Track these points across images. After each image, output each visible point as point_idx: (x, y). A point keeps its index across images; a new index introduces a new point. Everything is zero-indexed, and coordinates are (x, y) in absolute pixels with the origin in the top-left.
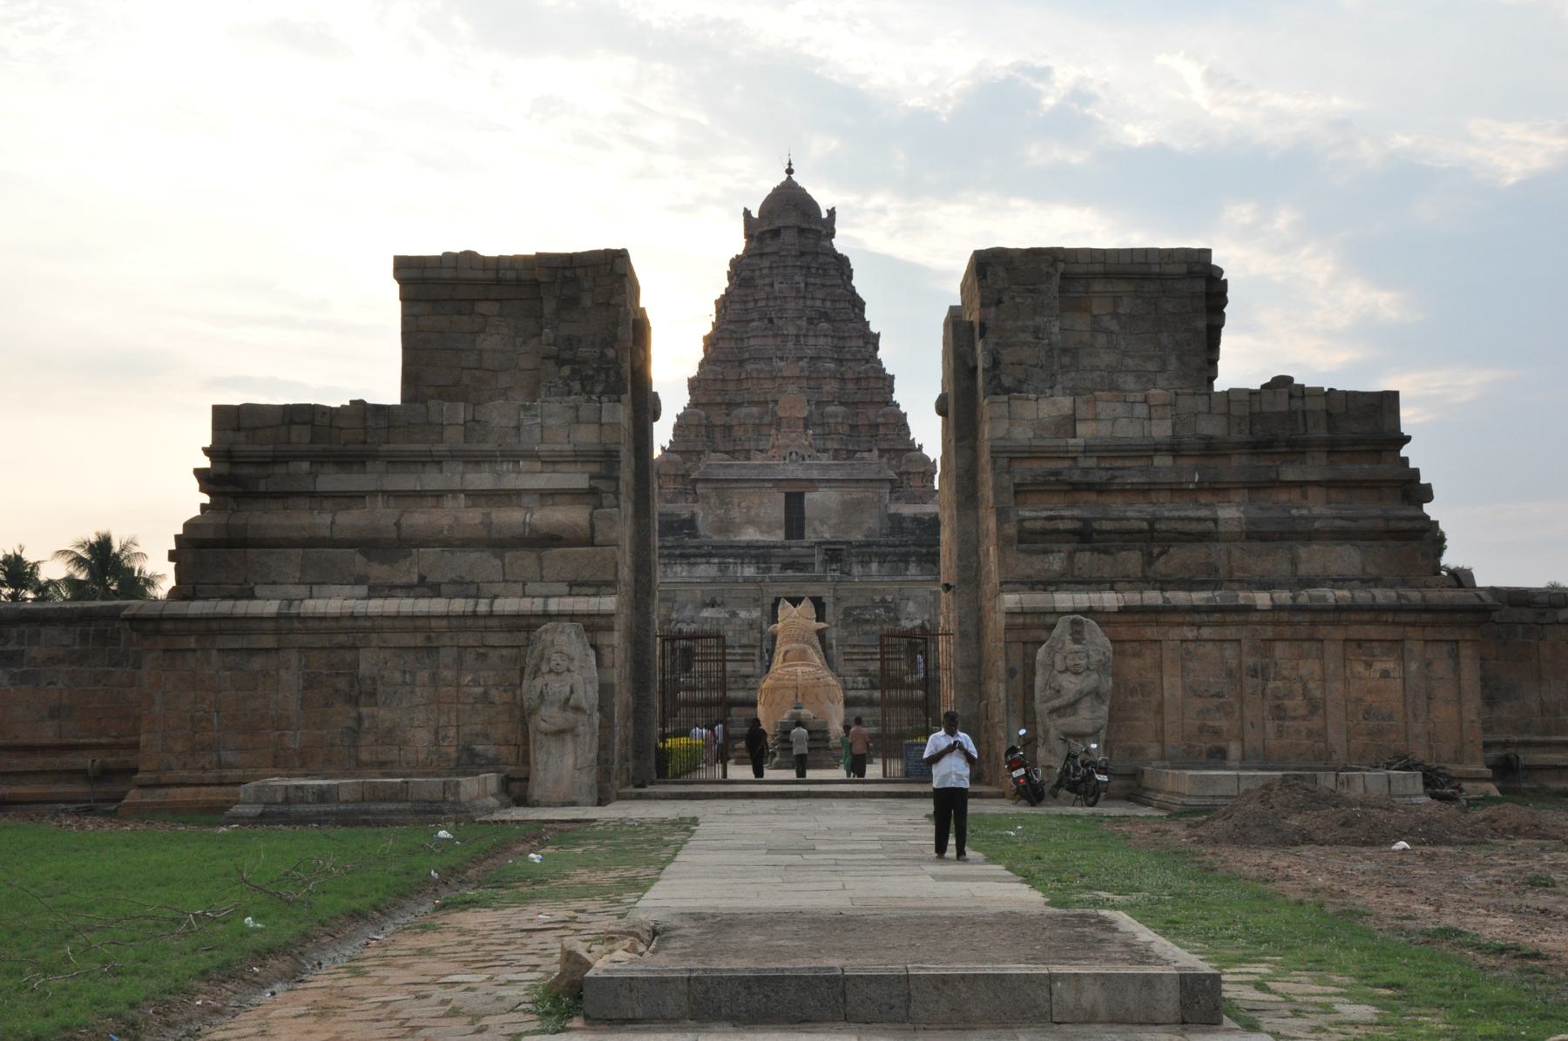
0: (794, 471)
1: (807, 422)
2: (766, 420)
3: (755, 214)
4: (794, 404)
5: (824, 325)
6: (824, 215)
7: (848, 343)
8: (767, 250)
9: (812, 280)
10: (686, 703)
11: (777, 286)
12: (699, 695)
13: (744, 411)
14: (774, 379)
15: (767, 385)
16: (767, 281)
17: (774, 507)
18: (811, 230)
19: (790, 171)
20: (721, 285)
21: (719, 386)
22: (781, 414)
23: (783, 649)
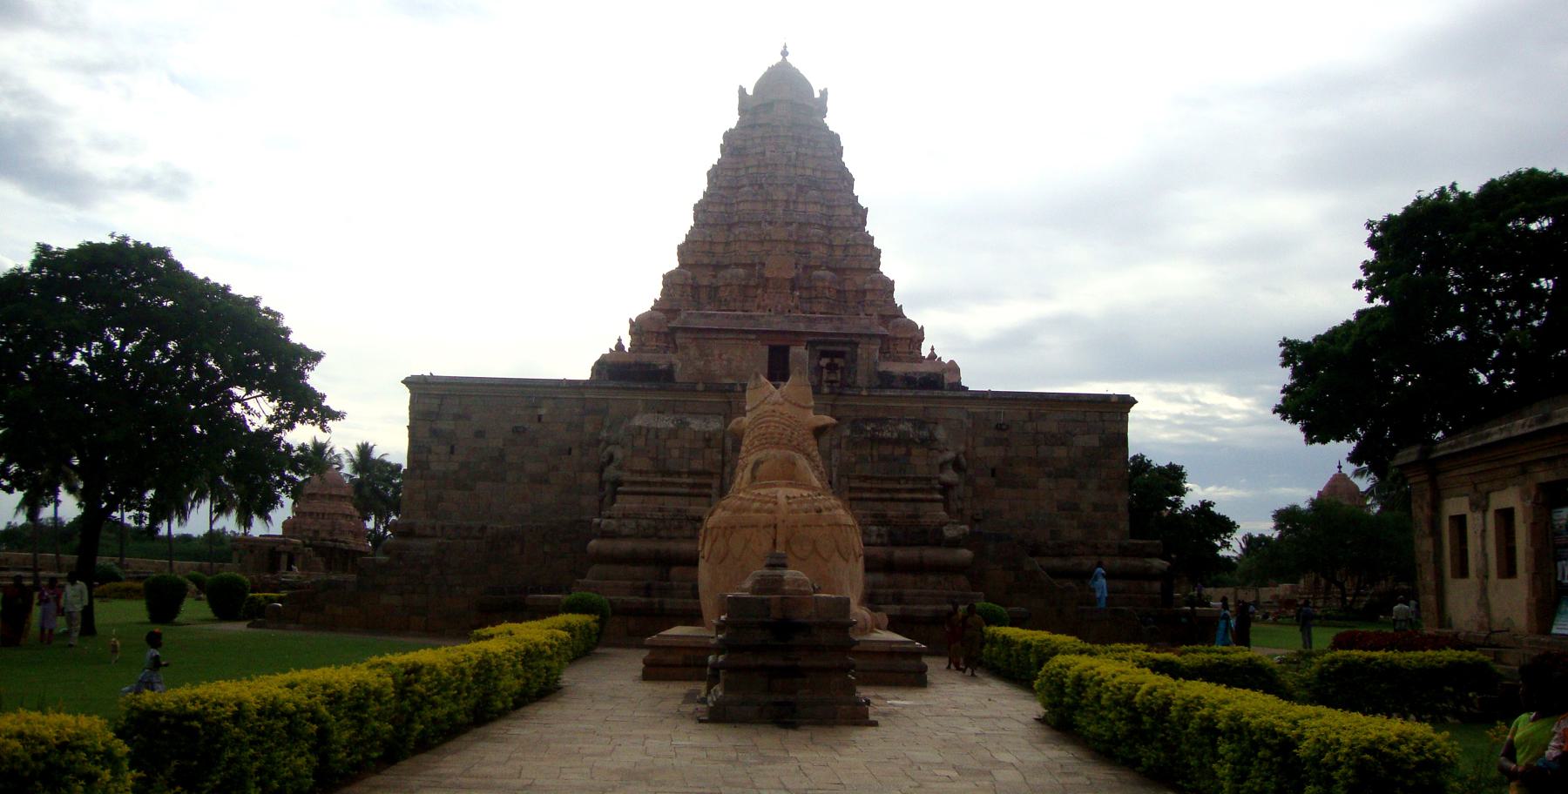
0: (779, 323)
1: (794, 284)
2: (752, 283)
3: (750, 92)
6: (817, 95)
9: (802, 150)
12: (625, 546)
13: (728, 273)
14: (762, 242)
15: (755, 248)
16: (759, 149)
19: (785, 53)
20: (714, 156)
21: (707, 247)
22: (767, 274)
23: (752, 458)
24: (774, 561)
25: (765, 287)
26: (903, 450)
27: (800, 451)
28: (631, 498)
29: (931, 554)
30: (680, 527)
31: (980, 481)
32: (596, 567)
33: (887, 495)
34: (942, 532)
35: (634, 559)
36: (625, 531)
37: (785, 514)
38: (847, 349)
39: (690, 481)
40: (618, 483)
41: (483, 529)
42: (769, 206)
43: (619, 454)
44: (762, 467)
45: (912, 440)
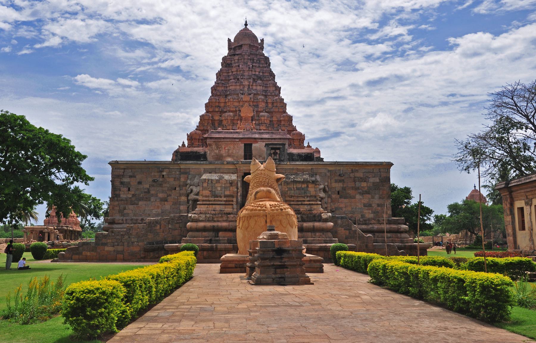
1: (253, 119)
2: (236, 118)
3: (232, 41)
4: (247, 112)
5: (259, 81)
6: (259, 41)
7: (269, 89)
8: (237, 53)
9: (254, 64)
10: (192, 230)
11: (240, 66)
12: (201, 224)
14: (239, 102)
15: (236, 104)
16: (237, 64)
17: (240, 150)
18: (254, 46)
22: (242, 115)
24: (270, 228)
25: (241, 120)
26: (306, 185)
27: (271, 188)
28: (203, 206)
29: (317, 224)
30: (222, 217)
31: (334, 196)
32: (190, 233)
33: (300, 203)
34: (321, 216)
35: (205, 229)
36: (201, 219)
37: (269, 211)
38: (281, 147)
39: (225, 199)
40: (195, 201)
41: (142, 220)
42: (242, 87)
43: (195, 189)
44: (259, 194)
45: (309, 182)
